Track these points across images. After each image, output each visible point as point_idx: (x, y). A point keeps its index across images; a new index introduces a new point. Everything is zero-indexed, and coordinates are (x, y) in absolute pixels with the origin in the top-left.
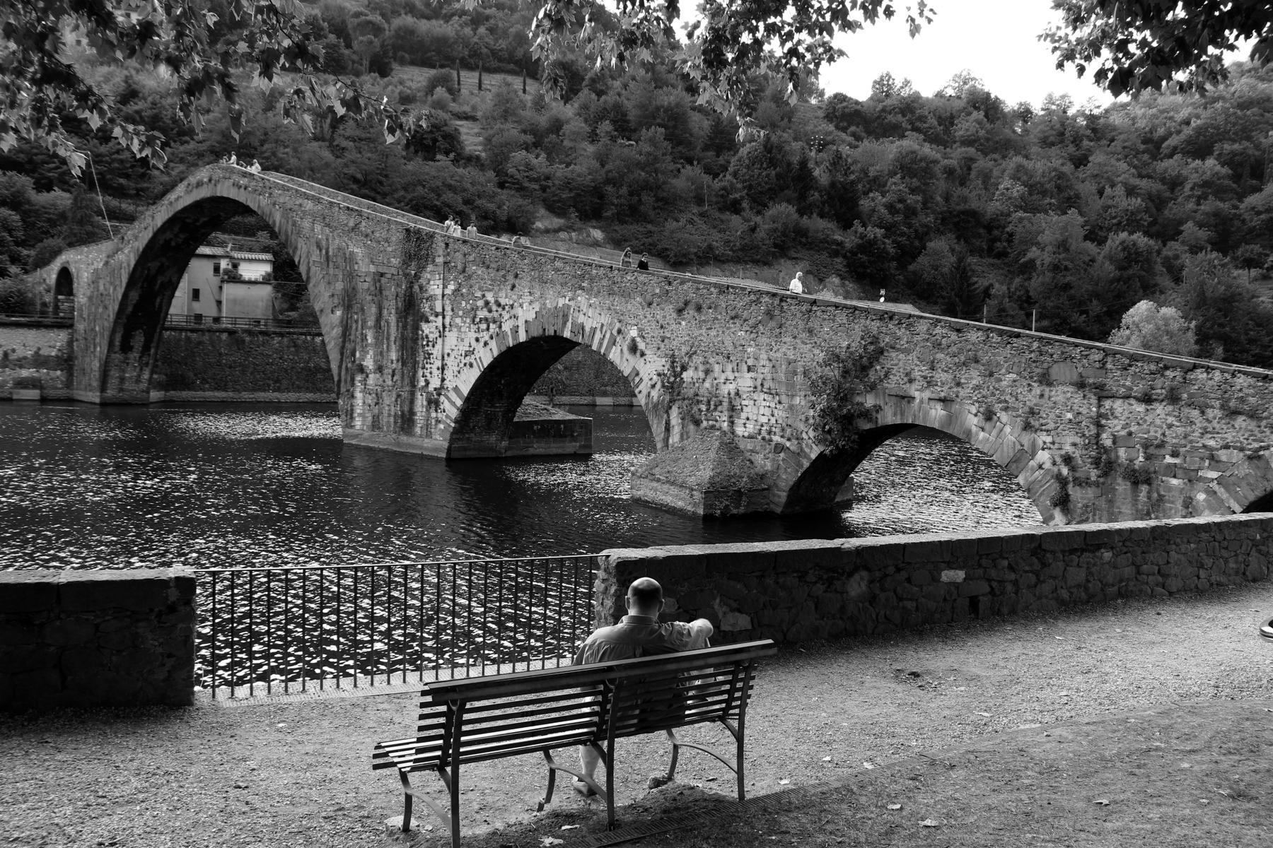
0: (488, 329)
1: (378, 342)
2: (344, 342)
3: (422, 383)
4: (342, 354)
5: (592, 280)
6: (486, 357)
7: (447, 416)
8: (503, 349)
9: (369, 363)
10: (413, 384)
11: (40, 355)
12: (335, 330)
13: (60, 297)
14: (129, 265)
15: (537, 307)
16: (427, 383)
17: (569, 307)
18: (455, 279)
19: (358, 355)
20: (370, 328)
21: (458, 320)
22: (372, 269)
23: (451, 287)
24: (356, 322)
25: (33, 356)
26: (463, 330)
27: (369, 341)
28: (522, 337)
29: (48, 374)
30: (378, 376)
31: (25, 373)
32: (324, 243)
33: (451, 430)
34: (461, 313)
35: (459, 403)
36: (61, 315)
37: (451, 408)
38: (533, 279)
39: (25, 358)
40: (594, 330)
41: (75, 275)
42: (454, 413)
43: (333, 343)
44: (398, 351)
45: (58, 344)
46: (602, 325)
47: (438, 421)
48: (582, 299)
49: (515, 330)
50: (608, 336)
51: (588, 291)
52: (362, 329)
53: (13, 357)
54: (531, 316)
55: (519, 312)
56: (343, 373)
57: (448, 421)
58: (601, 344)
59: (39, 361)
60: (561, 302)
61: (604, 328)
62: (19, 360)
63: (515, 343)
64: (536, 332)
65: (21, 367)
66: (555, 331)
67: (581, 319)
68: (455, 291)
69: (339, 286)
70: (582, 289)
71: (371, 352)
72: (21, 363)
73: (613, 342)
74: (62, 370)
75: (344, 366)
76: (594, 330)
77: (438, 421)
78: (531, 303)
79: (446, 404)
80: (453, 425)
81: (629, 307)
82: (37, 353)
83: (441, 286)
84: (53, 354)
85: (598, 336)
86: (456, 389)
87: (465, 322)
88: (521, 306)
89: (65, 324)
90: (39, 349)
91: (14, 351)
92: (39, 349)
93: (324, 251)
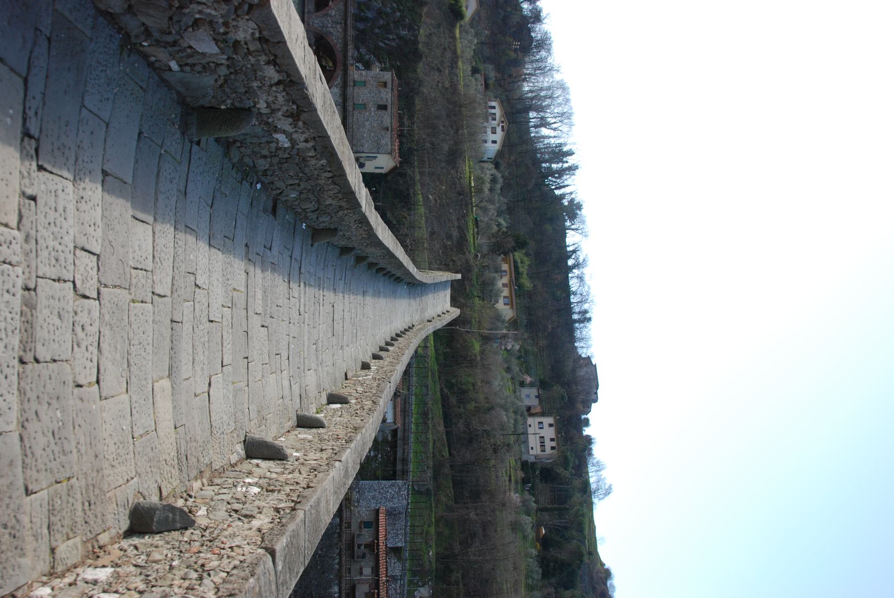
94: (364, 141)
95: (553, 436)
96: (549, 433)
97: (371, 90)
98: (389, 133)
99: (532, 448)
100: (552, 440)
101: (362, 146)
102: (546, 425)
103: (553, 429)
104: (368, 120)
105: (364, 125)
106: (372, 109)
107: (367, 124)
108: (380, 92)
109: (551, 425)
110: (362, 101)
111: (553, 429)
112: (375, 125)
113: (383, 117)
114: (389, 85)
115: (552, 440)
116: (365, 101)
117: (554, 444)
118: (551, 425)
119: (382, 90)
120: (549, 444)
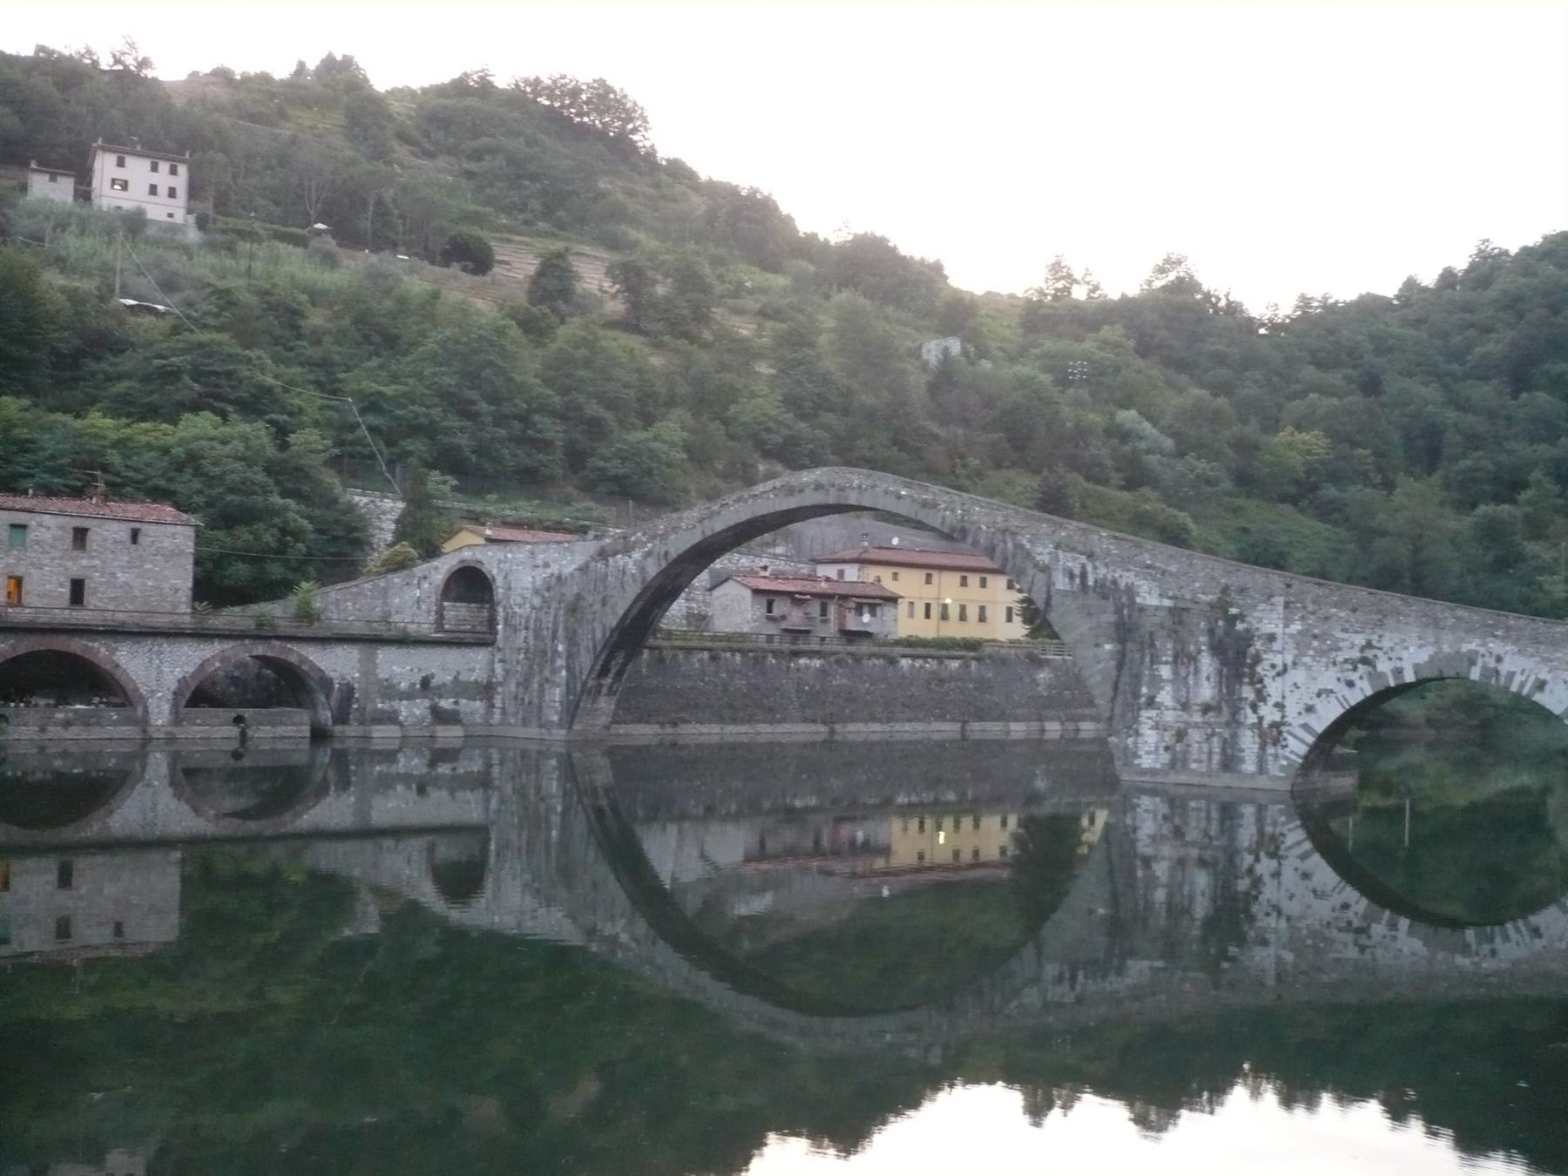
0: (1355, 669)
1: (1179, 680)
2: (1118, 676)
3: (1252, 718)
4: (1116, 689)
5: (1508, 629)
6: (1355, 697)
7: (1292, 752)
8: (1382, 688)
9: (1165, 697)
10: (1234, 722)
11: (460, 682)
12: (1101, 666)
13: (445, 604)
14: (642, 570)
15: (1430, 651)
16: (1261, 719)
17: (1476, 652)
18: (1303, 618)
19: (1144, 690)
20: (1166, 663)
21: (1307, 660)
22: (1168, 603)
23: (1296, 627)
24: (1142, 658)
25: (452, 683)
26: (1313, 668)
27: (1165, 677)
28: (1409, 677)
29: (467, 705)
30: (1181, 713)
31: (446, 704)
32: (1077, 571)
33: (1297, 766)
34: (1311, 652)
35: (1311, 739)
36: (447, 627)
37: (1297, 747)
38: (1427, 625)
39: (444, 685)
40: (1511, 675)
41: (499, 582)
42: (1303, 750)
43: (1099, 678)
44: (1214, 687)
45: (478, 666)
46: (1523, 671)
47: (1276, 756)
48: (1495, 646)
49: (1398, 672)
50: (1532, 678)
51: (1503, 639)
52: (1152, 662)
53: (434, 683)
54: (1423, 656)
55: (1404, 654)
56: (1118, 710)
57: (1294, 757)
58: (1522, 685)
59: (460, 688)
60: (1465, 648)
61: (1527, 672)
62: (438, 687)
63: (1400, 682)
64: (1427, 674)
65: (440, 696)
66: (1458, 674)
67: (1492, 663)
68: (1300, 632)
69: (1109, 618)
70: (1495, 636)
71: (1168, 688)
72: (440, 691)
73: (1541, 685)
74: (481, 700)
75: (1120, 699)
76: (1511, 675)
77: (1276, 756)
78: (1421, 646)
79: (1291, 741)
80: (1300, 761)
81: (1559, 655)
82: (456, 678)
83: (1281, 626)
84: (472, 679)
85: (1518, 679)
86: (1306, 727)
87: (1319, 662)
88: (1406, 648)
89: (484, 640)
90: (458, 673)
91: (433, 676)
92: (458, 673)
93: (1078, 581)
94: (166, 586)
95: (147, 163)
96: (138, 170)
97: (32, 564)
98: (144, 527)
99: (171, 215)
100: (154, 168)
101: (177, 591)
102: (121, 174)
103: (129, 160)
104: (113, 574)
105: (127, 583)
106: (85, 562)
107: (121, 577)
108: (37, 543)
109: (121, 163)
110: (61, 585)
111: (129, 160)
112: (126, 558)
113: (105, 540)
114: (21, 518)
115: (154, 168)
116: (62, 579)
117: (164, 167)
118: (121, 163)
119: (32, 535)
120: (163, 178)
